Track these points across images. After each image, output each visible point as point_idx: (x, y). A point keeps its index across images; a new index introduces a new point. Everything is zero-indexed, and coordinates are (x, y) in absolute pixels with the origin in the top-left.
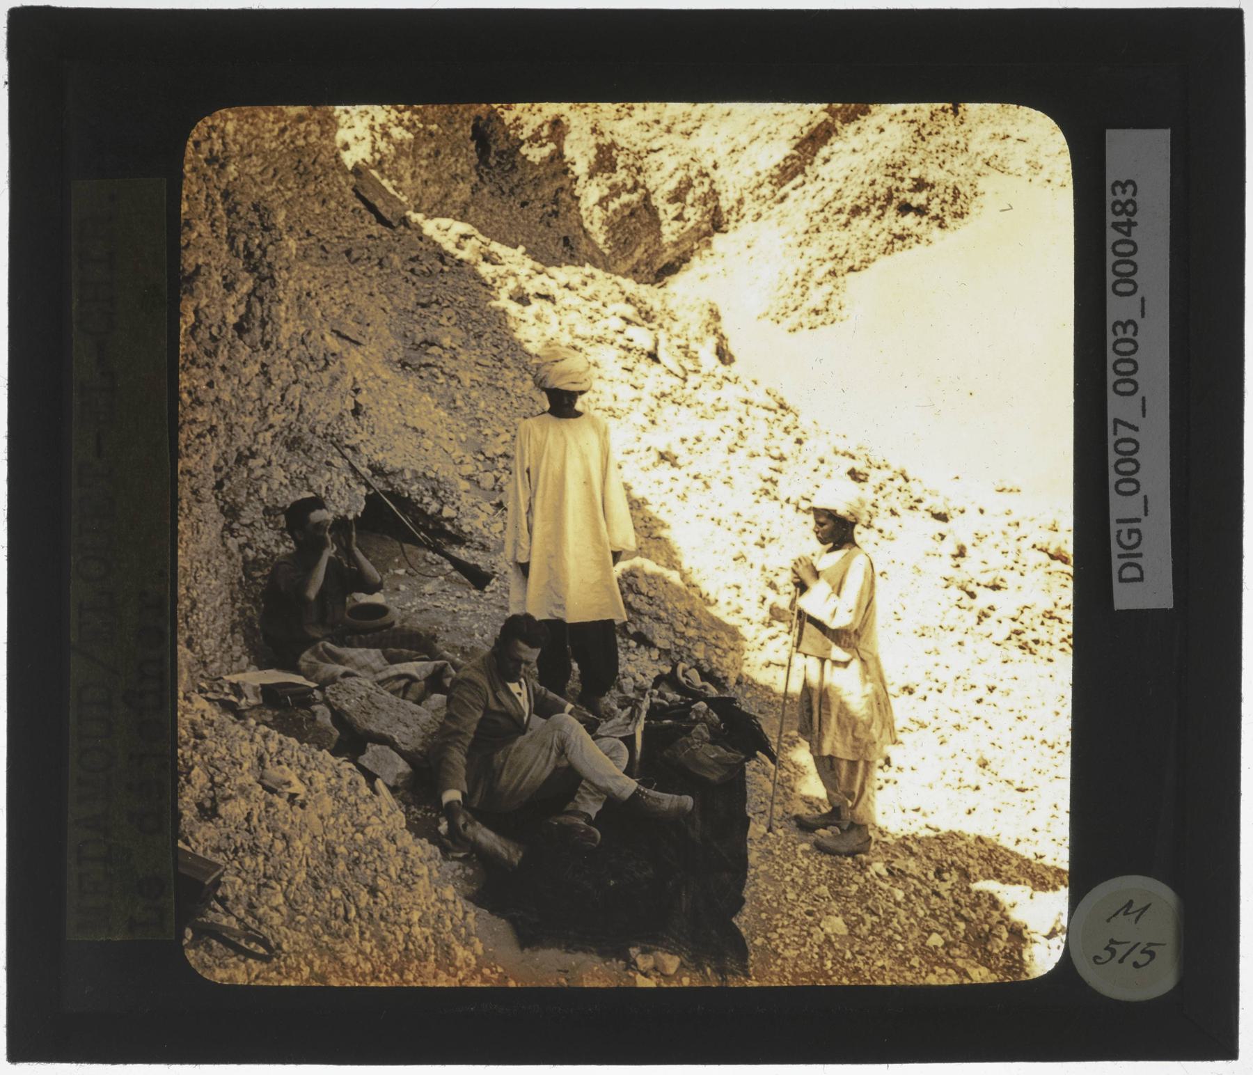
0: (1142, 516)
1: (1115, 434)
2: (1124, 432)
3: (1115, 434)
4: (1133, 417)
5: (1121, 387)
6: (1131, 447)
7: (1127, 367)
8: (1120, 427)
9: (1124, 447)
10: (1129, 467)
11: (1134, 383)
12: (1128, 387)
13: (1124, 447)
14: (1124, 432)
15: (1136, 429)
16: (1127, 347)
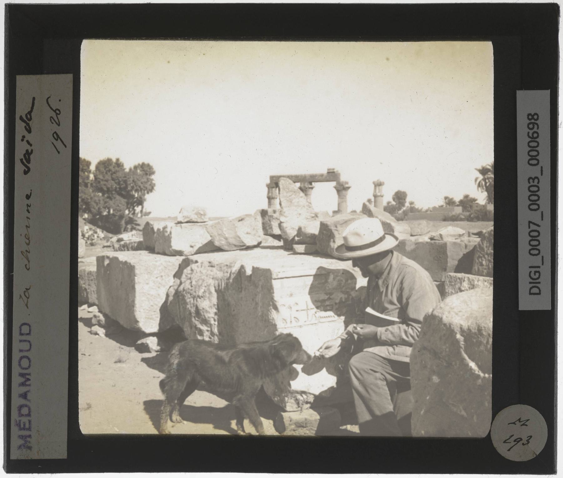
0: (540, 264)
1: (529, 227)
2: (533, 227)
3: (529, 228)
4: (537, 220)
5: (532, 207)
6: (535, 234)
7: (535, 198)
8: (531, 224)
9: (534, 234)
10: (534, 243)
11: (538, 205)
12: (535, 207)
13: (534, 234)
14: (533, 227)
15: (538, 226)
16: (535, 189)
